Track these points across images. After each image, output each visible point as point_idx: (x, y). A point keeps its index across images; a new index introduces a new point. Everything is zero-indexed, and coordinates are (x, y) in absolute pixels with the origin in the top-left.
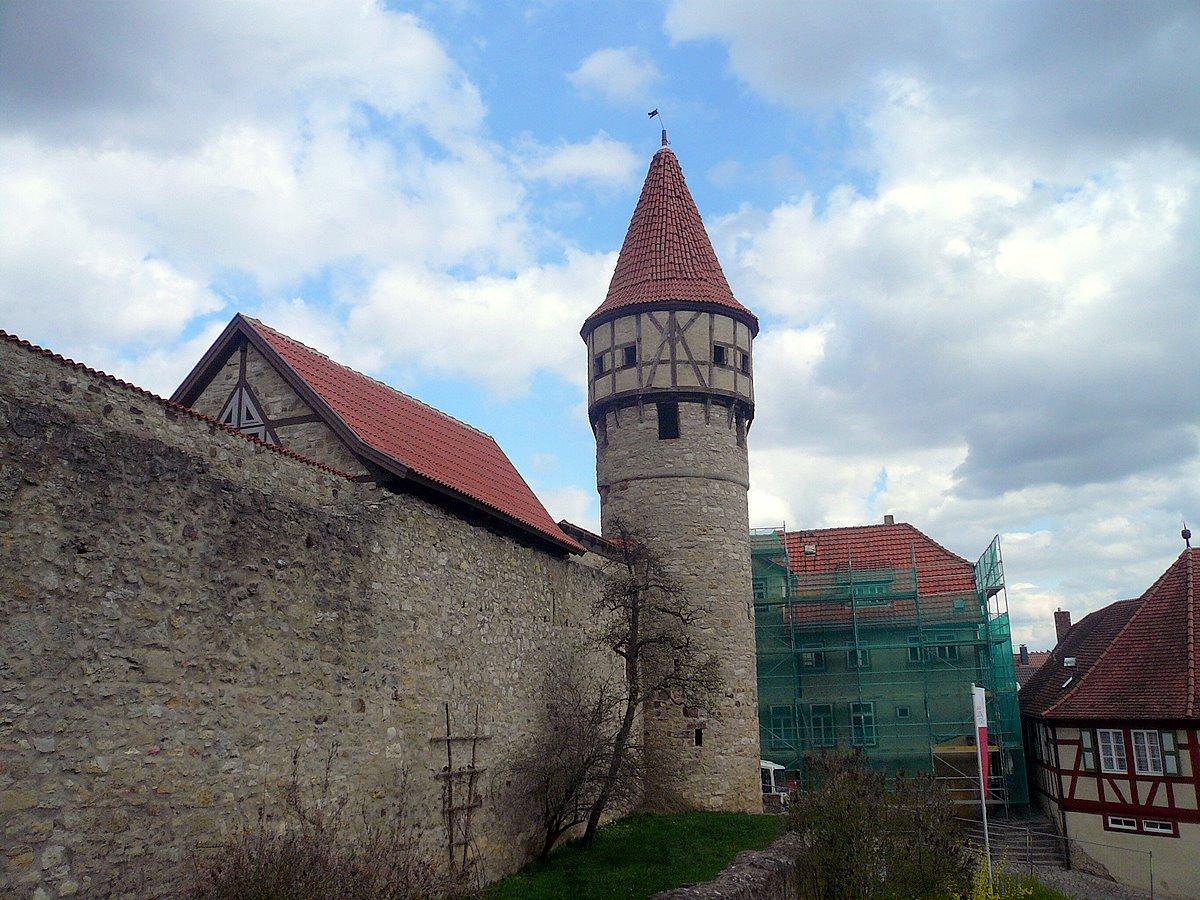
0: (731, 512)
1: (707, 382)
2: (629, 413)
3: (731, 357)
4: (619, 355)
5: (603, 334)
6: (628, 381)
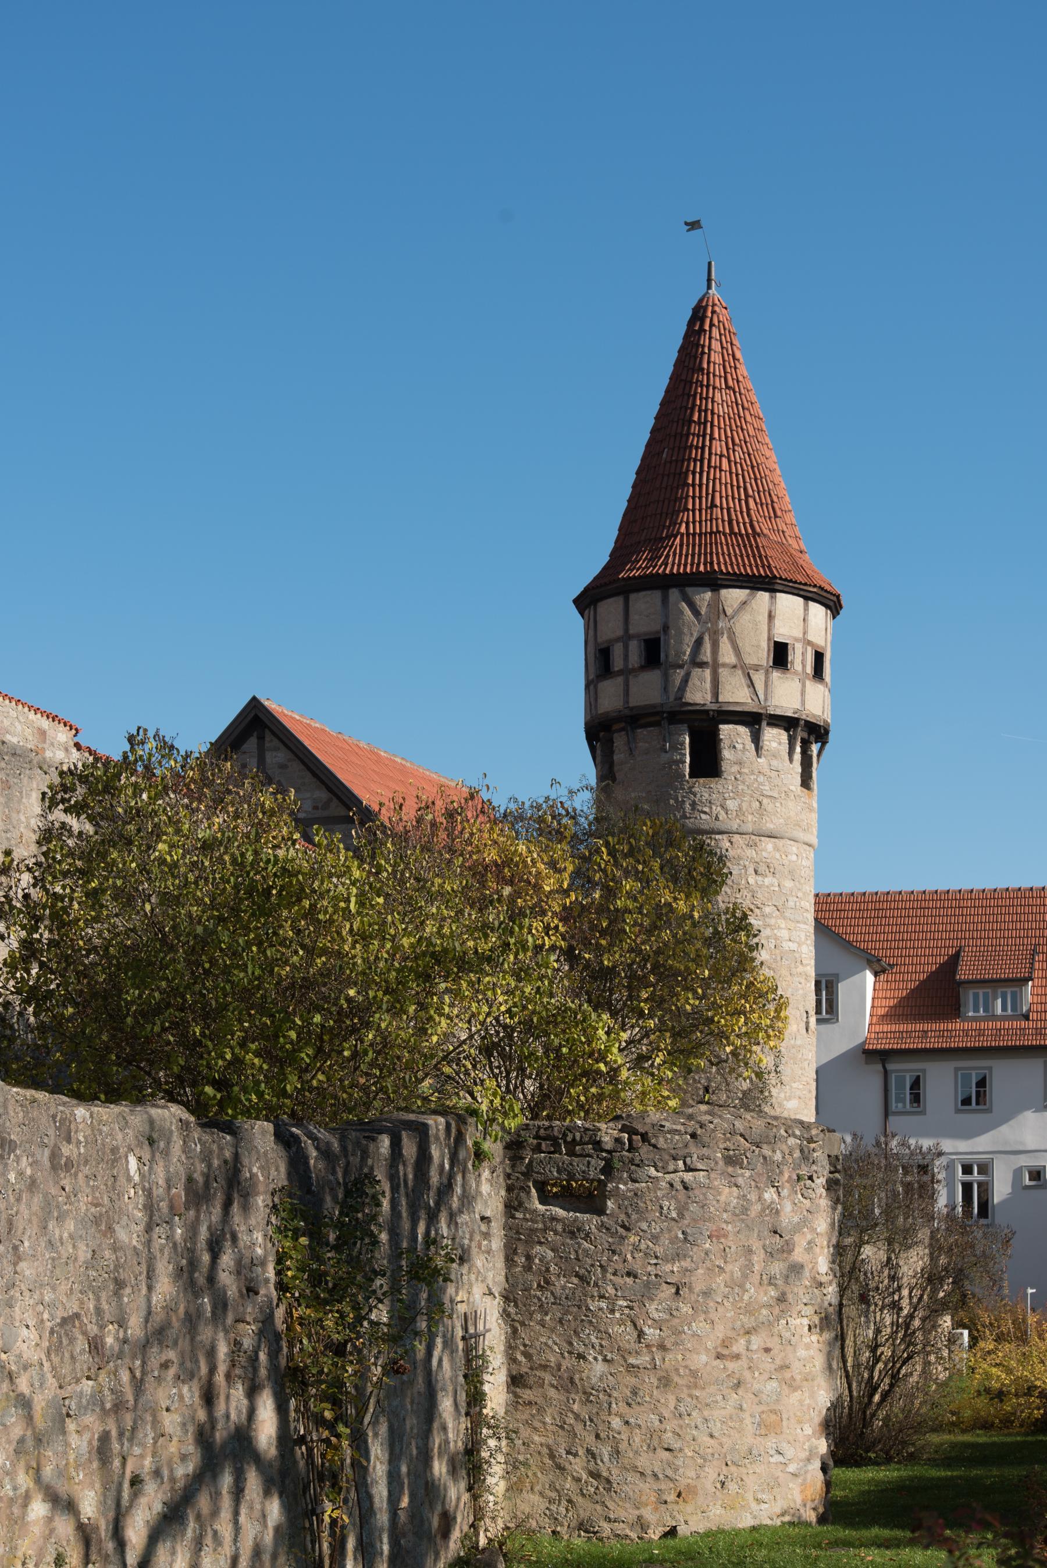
0: (788, 884)
1: (762, 697)
2: (646, 738)
3: (800, 659)
4: (634, 646)
5: (610, 609)
6: (647, 690)
